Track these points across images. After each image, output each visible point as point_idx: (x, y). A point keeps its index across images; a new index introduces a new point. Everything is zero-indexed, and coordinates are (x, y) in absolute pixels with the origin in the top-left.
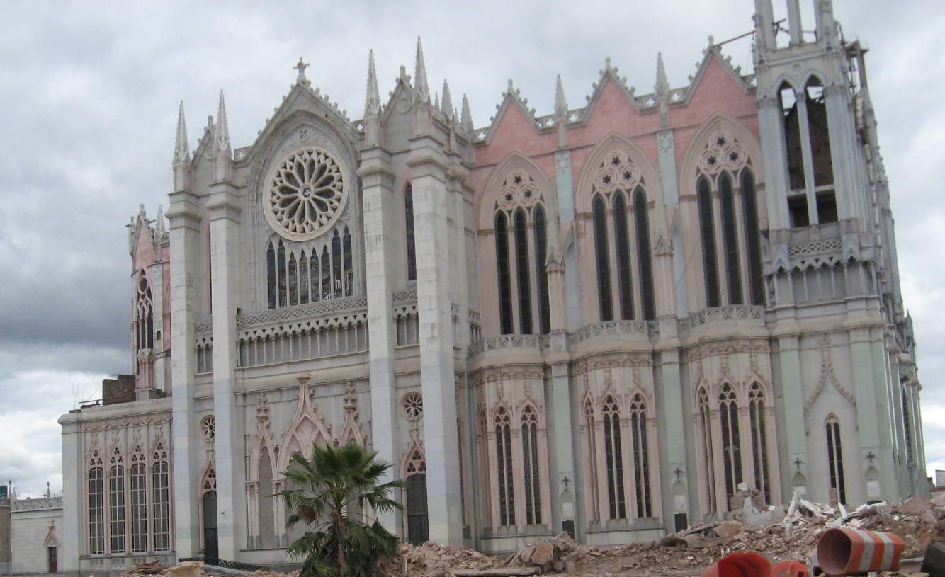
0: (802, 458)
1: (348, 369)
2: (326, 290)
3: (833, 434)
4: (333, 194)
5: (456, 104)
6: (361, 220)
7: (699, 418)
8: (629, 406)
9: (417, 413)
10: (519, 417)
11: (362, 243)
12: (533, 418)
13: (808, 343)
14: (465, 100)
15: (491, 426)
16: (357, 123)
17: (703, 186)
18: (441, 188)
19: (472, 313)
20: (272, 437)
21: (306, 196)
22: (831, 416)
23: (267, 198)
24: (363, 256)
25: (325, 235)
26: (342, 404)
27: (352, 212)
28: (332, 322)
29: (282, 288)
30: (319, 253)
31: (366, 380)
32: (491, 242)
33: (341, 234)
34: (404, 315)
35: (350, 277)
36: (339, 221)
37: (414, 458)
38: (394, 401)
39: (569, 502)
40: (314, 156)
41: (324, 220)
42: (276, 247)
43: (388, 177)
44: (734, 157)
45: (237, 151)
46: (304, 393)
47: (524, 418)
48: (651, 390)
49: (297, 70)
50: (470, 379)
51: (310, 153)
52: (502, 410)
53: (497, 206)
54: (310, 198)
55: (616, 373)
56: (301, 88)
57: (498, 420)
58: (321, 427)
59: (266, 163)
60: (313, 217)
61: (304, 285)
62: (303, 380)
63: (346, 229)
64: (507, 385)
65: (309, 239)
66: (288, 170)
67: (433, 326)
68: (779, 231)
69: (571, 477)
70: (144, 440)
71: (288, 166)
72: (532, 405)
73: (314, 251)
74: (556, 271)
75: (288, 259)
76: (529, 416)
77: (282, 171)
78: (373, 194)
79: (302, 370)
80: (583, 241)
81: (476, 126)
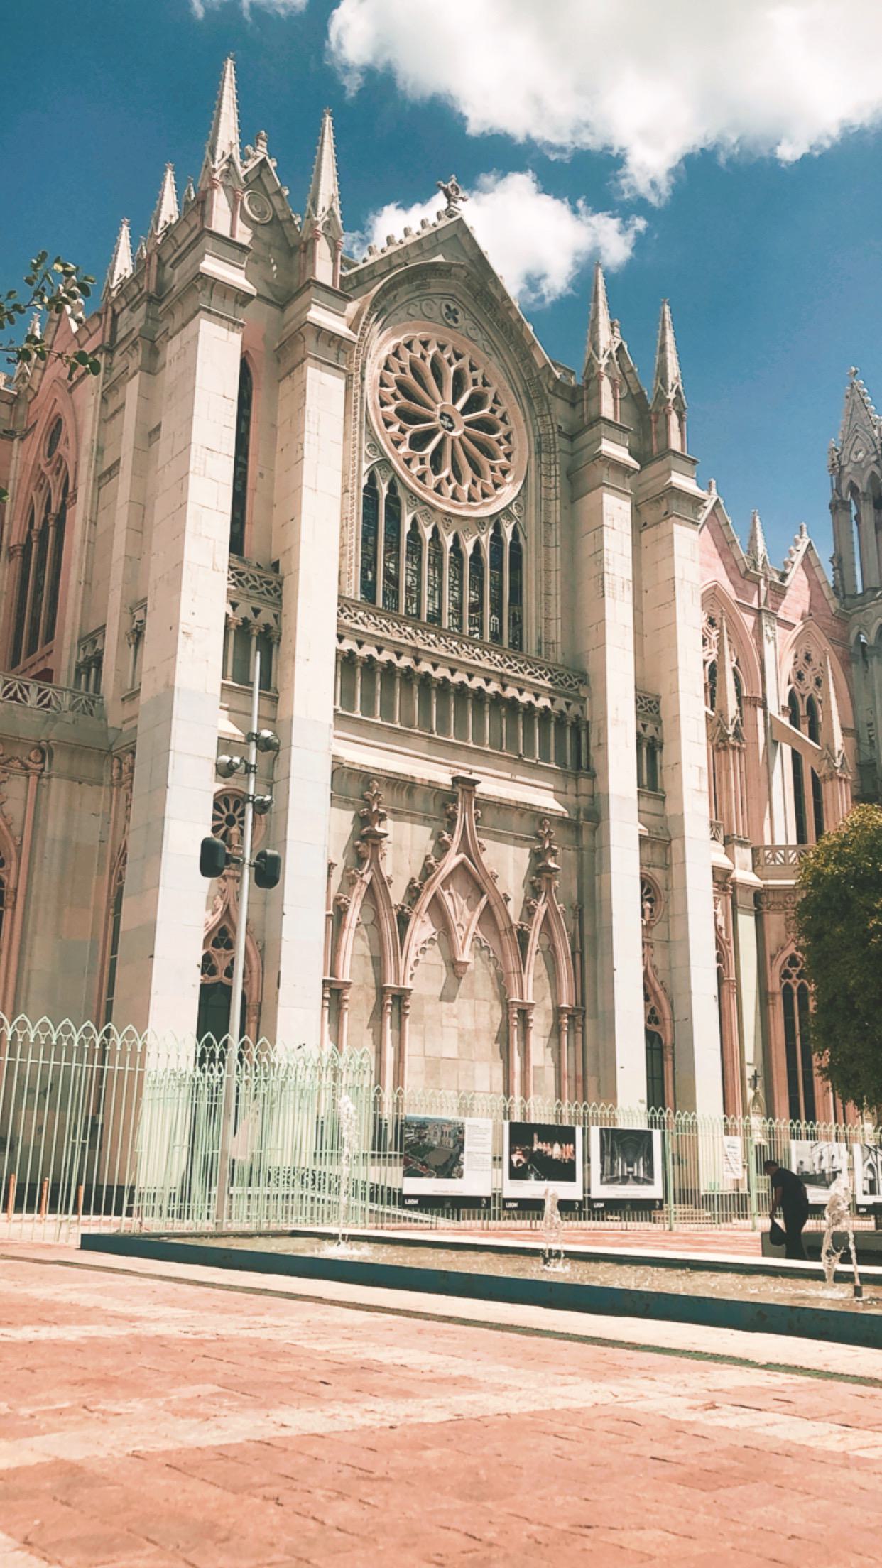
25: (480, 522)
35: (517, 622)
36: (506, 511)
42: (383, 489)
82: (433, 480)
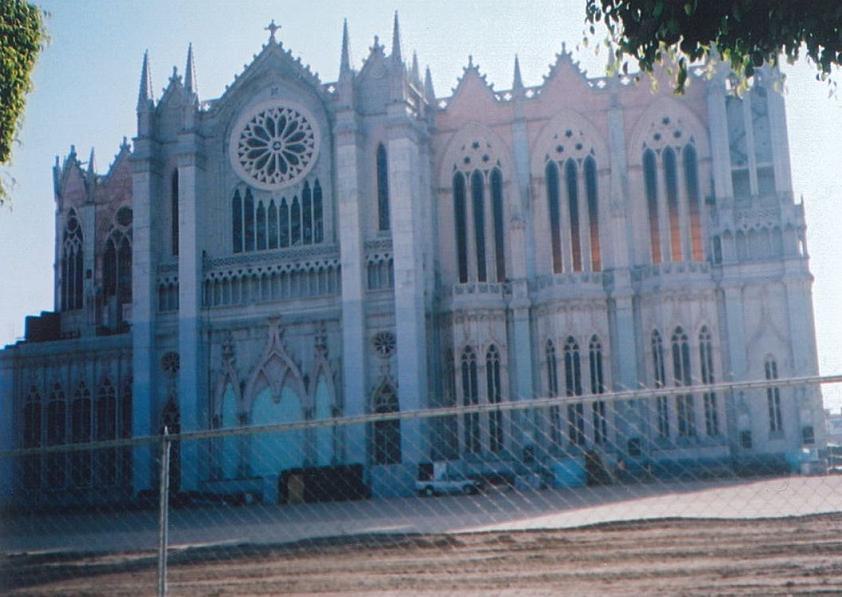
1: (320, 307)
2: (296, 236)
4: (304, 149)
5: (422, 75)
6: (333, 173)
7: (651, 356)
8: (588, 345)
9: (387, 351)
11: (334, 194)
14: (428, 71)
16: (327, 86)
17: (649, 158)
18: (416, 148)
19: (436, 263)
21: (275, 149)
23: (233, 149)
24: (335, 208)
26: (312, 342)
27: (324, 168)
28: (303, 265)
29: (249, 233)
30: (289, 203)
31: (337, 320)
32: (448, 201)
33: (312, 186)
34: (376, 261)
35: (320, 226)
36: (310, 174)
37: (384, 392)
38: (366, 339)
40: (285, 112)
41: (295, 172)
42: (243, 195)
43: (362, 135)
44: (677, 135)
45: (205, 102)
46: (274, 331)
48: (606, 331)
49: (269, 32)
50: (438, 319)
51: (281, 110)
52: (468, 349)
53: (455, 168)
54: (283, 148)
55: (577, 317)
56: (273, 50)
57: (464, 357)
58: (290, 363)
59: (235, 114)
60: (283, 169)
61: (273, 230)
62: (273, 319)
63: (317, 182)
64: (474, 326)
65: (281, 188)
66: (258, 124)
67: (408, 272)
68: (725, 199)
70: (114, 372)
71: (258, 121)
72: (495, 344)
73: (284, 200)
74: (518, 228)
75: (256, 206)
77: (252, 125)
78: (347, 151)
79: (269, 310)
80: (536, 201)
81: (438, 95)
82: (268, 179)
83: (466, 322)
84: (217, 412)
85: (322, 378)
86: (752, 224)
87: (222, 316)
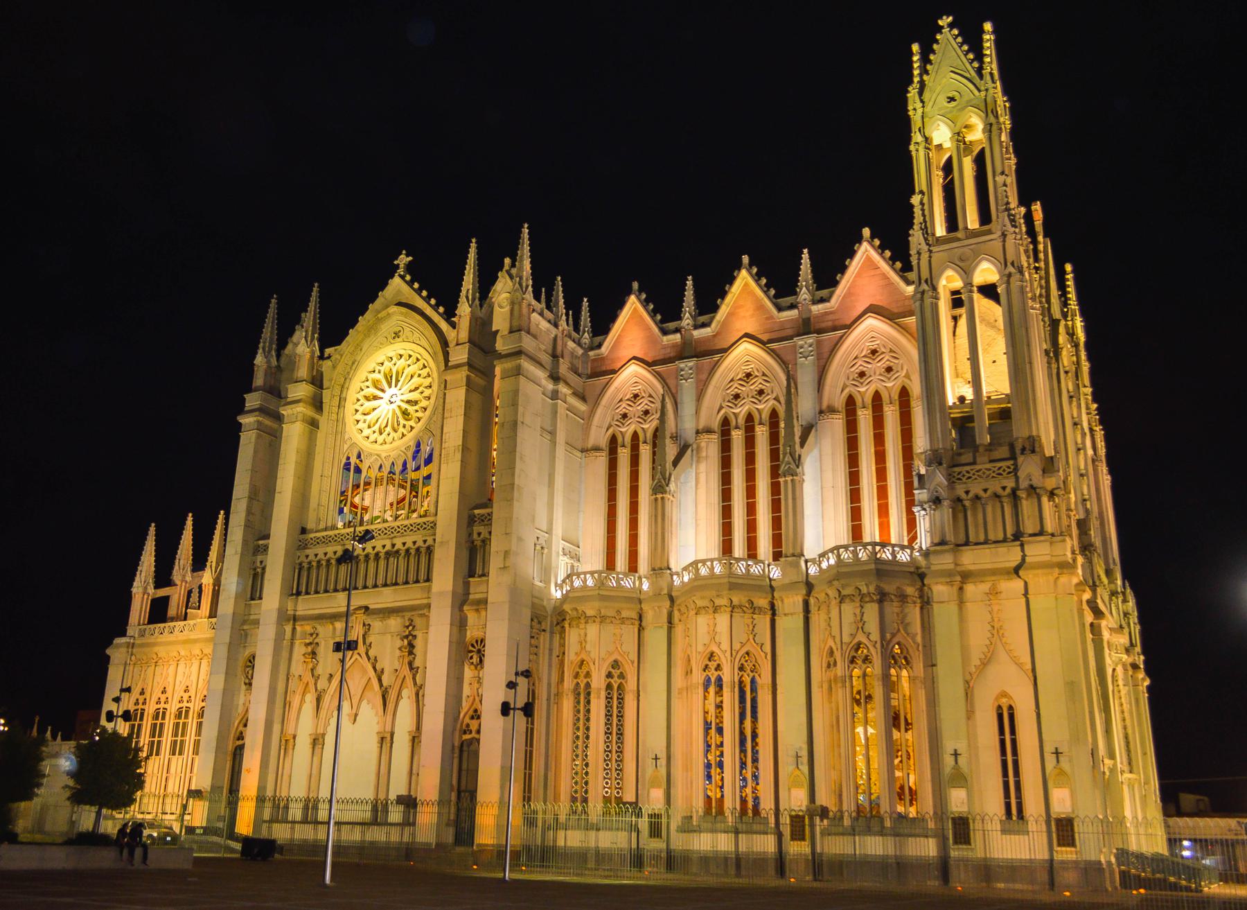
0: (962, 747)
3: (1006, 720)
10: (604, 674)
12: (622, 676)
13: (970, 588)
15: (568, 683)
20: (317, 679)
22: (1004, 694)
37: (472, 718)
39: (659, 787)
47: (609, 675)
57: (577, 675)
69: (663, 755)
76: (616, 673)
83: (582, 626)
84: (291, 731)
85: (405, 693)
86: (976, 489)
87: (307, 606)
